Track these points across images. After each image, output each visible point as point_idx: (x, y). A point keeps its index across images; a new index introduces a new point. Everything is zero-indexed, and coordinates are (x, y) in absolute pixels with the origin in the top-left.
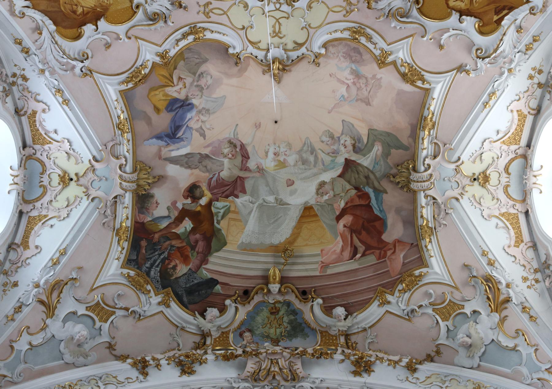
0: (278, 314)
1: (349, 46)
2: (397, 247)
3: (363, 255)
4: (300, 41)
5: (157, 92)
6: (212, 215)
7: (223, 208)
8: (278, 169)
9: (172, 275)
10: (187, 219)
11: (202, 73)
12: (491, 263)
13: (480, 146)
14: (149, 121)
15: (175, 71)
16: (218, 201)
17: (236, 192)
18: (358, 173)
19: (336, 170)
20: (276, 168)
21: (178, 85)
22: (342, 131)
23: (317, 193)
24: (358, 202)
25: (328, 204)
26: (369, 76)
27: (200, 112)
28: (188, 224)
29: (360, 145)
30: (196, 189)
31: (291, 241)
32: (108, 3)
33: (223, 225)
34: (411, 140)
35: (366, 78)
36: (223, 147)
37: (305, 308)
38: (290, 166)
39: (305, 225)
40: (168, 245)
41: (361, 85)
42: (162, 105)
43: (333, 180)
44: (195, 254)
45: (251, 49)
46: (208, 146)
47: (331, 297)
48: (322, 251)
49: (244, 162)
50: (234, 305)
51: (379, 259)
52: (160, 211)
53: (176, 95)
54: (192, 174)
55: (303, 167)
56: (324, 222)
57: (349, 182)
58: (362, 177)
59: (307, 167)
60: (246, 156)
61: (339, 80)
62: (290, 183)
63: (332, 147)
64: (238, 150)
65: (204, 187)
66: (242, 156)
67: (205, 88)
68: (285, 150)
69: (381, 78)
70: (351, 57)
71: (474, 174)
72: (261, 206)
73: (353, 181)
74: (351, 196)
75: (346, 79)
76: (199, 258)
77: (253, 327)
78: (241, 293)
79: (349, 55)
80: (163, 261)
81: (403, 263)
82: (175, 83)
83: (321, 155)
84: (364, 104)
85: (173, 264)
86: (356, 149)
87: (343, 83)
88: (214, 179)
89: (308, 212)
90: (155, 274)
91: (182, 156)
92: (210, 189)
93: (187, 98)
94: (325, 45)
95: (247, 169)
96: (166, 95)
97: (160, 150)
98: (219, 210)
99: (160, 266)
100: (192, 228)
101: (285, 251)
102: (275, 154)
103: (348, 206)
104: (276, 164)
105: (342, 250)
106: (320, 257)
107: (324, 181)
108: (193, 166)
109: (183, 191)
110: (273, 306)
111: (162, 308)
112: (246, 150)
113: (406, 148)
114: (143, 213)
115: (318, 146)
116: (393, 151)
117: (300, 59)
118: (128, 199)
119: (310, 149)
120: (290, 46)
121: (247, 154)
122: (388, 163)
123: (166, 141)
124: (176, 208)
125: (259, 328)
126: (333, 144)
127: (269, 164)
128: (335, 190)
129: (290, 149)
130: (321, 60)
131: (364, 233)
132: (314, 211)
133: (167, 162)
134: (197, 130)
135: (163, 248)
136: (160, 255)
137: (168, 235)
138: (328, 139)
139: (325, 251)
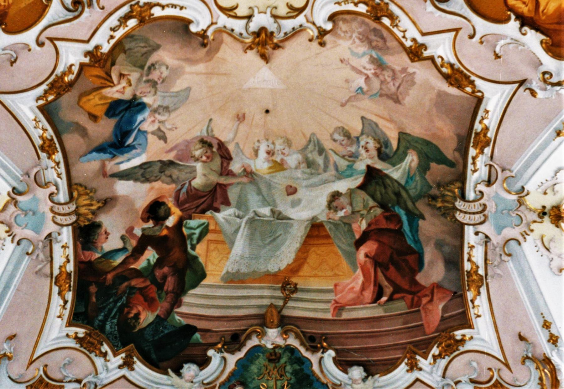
0: (279, 361)
2: (435, 294)
3: (391, 299)
5: (91, 97)
6: (183, 239)
7: (198, 227)
8: (273, 172)
9: (135, 327)
10: (149, 248)
11: (153, 65)
14: (83, 132)
15: (113, 68)
16: (190, 218)
17: (215, 205)
18: (385, 188)
19: (356, 179)
20: (271, 170)
21: (119, 83)
22: (362, 130)
23: (329, 206)
24: (384, 225)
25: (345, 224)
26: (398, 68)
27: (155, 111)
28: (151, 255)
29: (387, 151)
30: (160, 207)
31: (295, 268)
32: (6, 4)
33: (200, 251)
34: (457, 154)
35: (393, 71)
36: (192, 148)
37: (314, 358)
38: (291, 168)
39: (313, 249)
40: (127, 287)
41: (387, 78)
42: (100, 111)
43: (351, 192)
44: (164, 294)
45: (223, 20)
46: (171, 150)
47: (348, 349)
48: (336, 285)
49: (225, 164)
50: (219, 355)
51: (411, 306)
52: (112, 243)
53: (117, 96)
54: (152, 188)
55: (308, 170)
56: (339, 246)
57: (373, 197)
58: (390, 192)
59: (313, 171)
60: (226, 157)
61: (354, 68)
62: (291, 191)
63: (349, 149)
64: (215, 150)
65: (170, 203)
66: (222, 157)
67: (159, 82)
68: (282, 147)
69: (414, 73)
70: (370, 42)
71: (544, 207)
72: (251, 221)
73: (378, 195)
74: (375, 216)
75: (364, 68)
76: (169, 299)
77: (246, 379)
78: (228, 339)
79: (367, 38)
81: (442, 317)
82: (115, 81)
83: (334, 158)
84: (390, 103)
85: (134, 312)
86: (382, 156)
87: (360, 72)
88: (184, 190)
89: (316, 231)
90: (111, 328)
91: (135, 168)
92: (179, 203)
93: (135, 97)
94: (332, 18)
95: (230, 174)
96: (104, 98)
97: (103, 166)
98: (193, 231)
99: (117, 317)
100: (158, 260)
101: (287, 284)
102: (268, 153)
103: (371, 229)
104: (270, 165)
105: (363, 289)
106: (333, 294)
107: (338, 192)
108: (153, 178)
109: (141, 212)
110: (272, 351)
111: (125, 371)
112: (227, 150)
113: (451, 164)
114: (89, 249)
115: (328, 145)
116: (433, 165)
117: (296, 32)
118: (66, 236)
119: (317, 148)
120: (283, 11)
121: (229, 154)
122: (425, 179)
123: (110, 153)
124: (134, 236)
125: (254, 379)
126: (351, 145)
127: (261, 165)
128: (354, 205)
129: (290, 146)
130: (327, 38)
131: (392, 269)
132: (326, 231)
133: (116, 179)
134: (153, 133)
135: (120, 292)
136: (116, 302)
137: (126, 274)
138: (342, 138)
139: (339, 286)
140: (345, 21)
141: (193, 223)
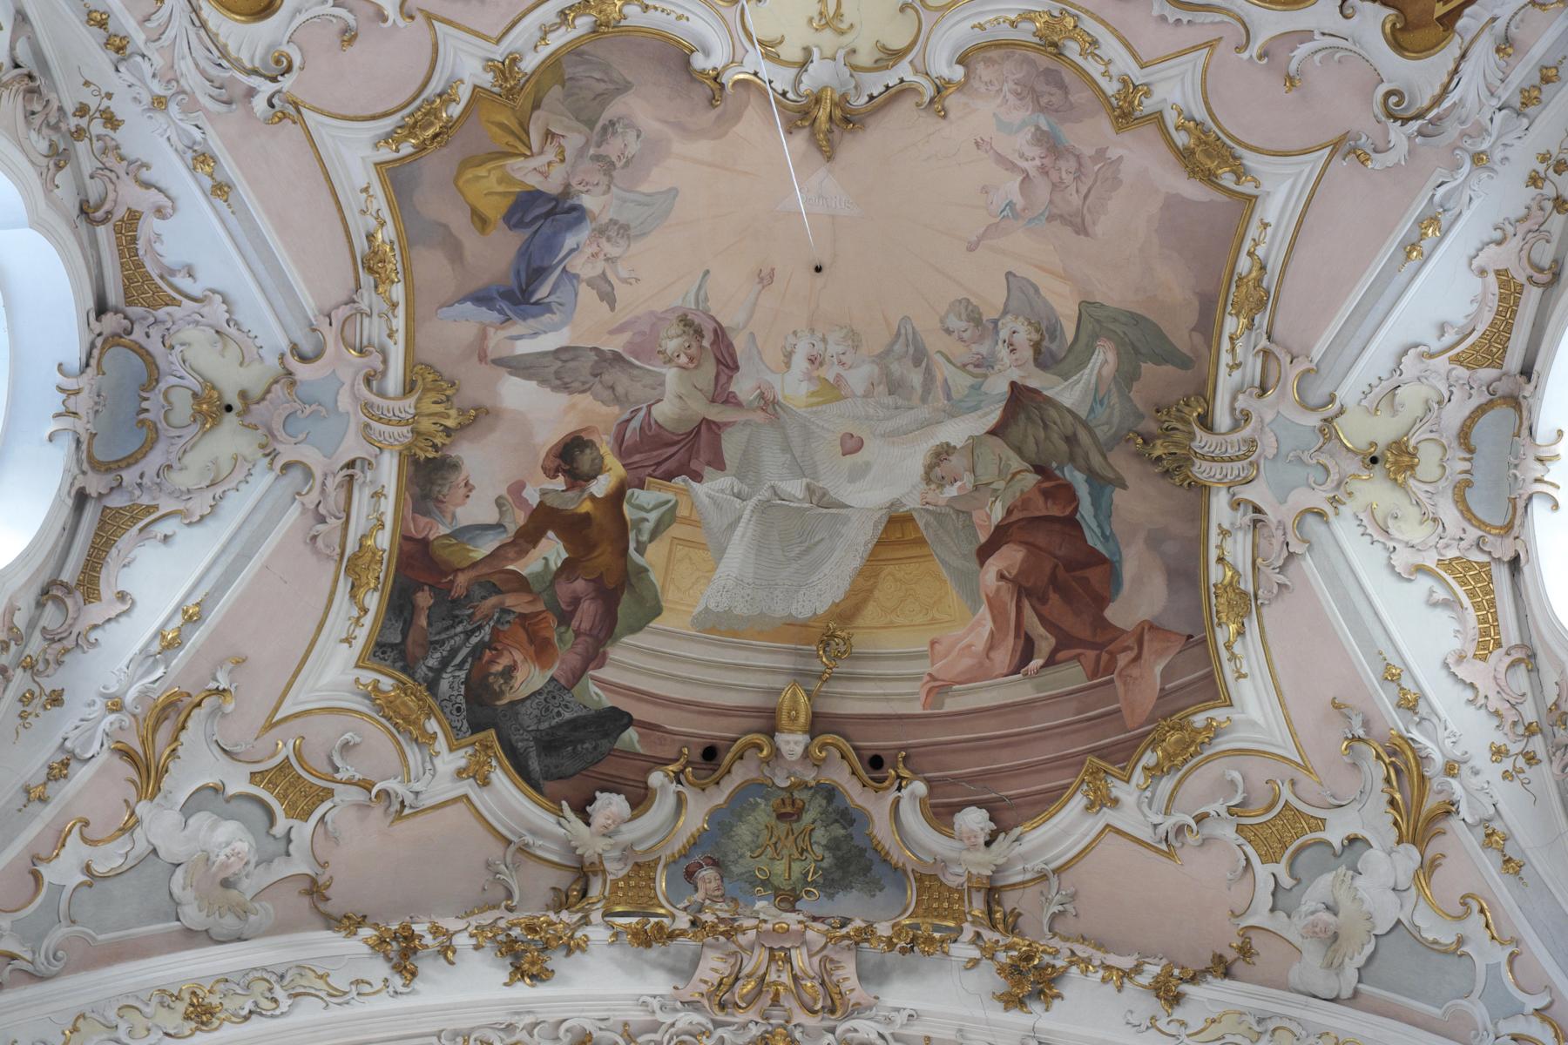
0: (798, 820)
1: (1032, 63)
2: (1146, 644)
3: (1050, 662)
4: (897, 44)
5: (482, 171)
6: (622, 525)
7: (656, 507)
8: (818, 404)
9: (502, 693)
10: (550, 534)
11: (612, 123)
12: (1410, 704)
13: (1391, 365)
14: (454, 250)
15: (536, 114)
16: (641, 487)
17: (694, 465)
18: (1046, 427)
19: (986, 415)
20: (815, 400)
21: (541, 152)
22: (1006, 305)
23: (928, 479)
24: (1041, 508)
25: (958, 512)
26: (1088, 151)
27: (601, 231)
28: (552, 551)
29: (1054, 347)
30: (582, 451)
31: (847, 612)
33: (653, 558)
34: (1198, 338)
35: (1078, 157)
36: (663, 334)
37: (875, 806)
38: (855, 395)
39: (890, 569)
40: (494, 607)
41: (1064, 175)
42: (495, 209)
43: (974, 444)
44: (570, 635)
45: (754, 61)
46: (620, 329)
47: (954, 777)
48: (933, 643)
49: (723, 379)
50: (674, 787)
51: (1094, 674)
52: (476, 509)
53: (534, 181)
54: (573, 406)
55: (889, 400)
56: (943, 562)
57: (1019, 451)
58: (1055, 437)
59: (900, 402)
60: (727, 363)
61: (1001, 159)
62: (852, 445)
63: (975, 348)
64: (706, 343)
65: (606, 448)
66: (718, 361)
67: (618, 165)
68: (840, 349)
69: (1121, 157)
70: (1036, 96)
72: (764, 508)
73: (1030, 447)
74: (1022, 492)
75: (1022, 156)
76: (579, 649)
77: (726, 855)
78: (697, 755)
79: (1033, 90)
80: (476, 653)
81: (1162, 689)
82: (535, 148)
83: (944, 370)
84: (1068, 231)
85: (504, 661)
86: (1043, 358)
87: (1012, 167)
88: (635, 424)
89: (898, 531)
90: (451, 687)
91: (545, 354)
92: (622, 451)
93: (567, 192)
95: (730, 400)
96: (505, 179)
97: (483, 336)
98: (644, 515)
99: (467, 666)
100: (566, 562)
101: (829, 640)
102: (812, 361)
103: (1013, 518)
104: (813, 389)
105: (992, 646)
106: (928, 662)
107: (948, 444)
108: (576, 385)
109: (543, 455)
110: (785, 795)
111: (467, 787)
112: (730, 345)
113: (1184, 362)
114: (427, 513)
115: (934, 342)
116: (1147, 367)
118: (388, 471)
119: (911, 350)
121: (733, 356)
122: (1130, 400)
123: (500, 312)
124: (522, 502)
125: (741, 856)
126: (980, 339)
127: (794, 388)
128: (979, 471)
129: (856, 348)
131: (1054, 598)
132: (916, 528)
133: (503, 371)
134: (590, 283)
135: (478, 616)
136: (469, 634)
137: (497, 579)
138: (964, 325)
139: (940, 644)
140: (989, 62)
141: (645, 497)
